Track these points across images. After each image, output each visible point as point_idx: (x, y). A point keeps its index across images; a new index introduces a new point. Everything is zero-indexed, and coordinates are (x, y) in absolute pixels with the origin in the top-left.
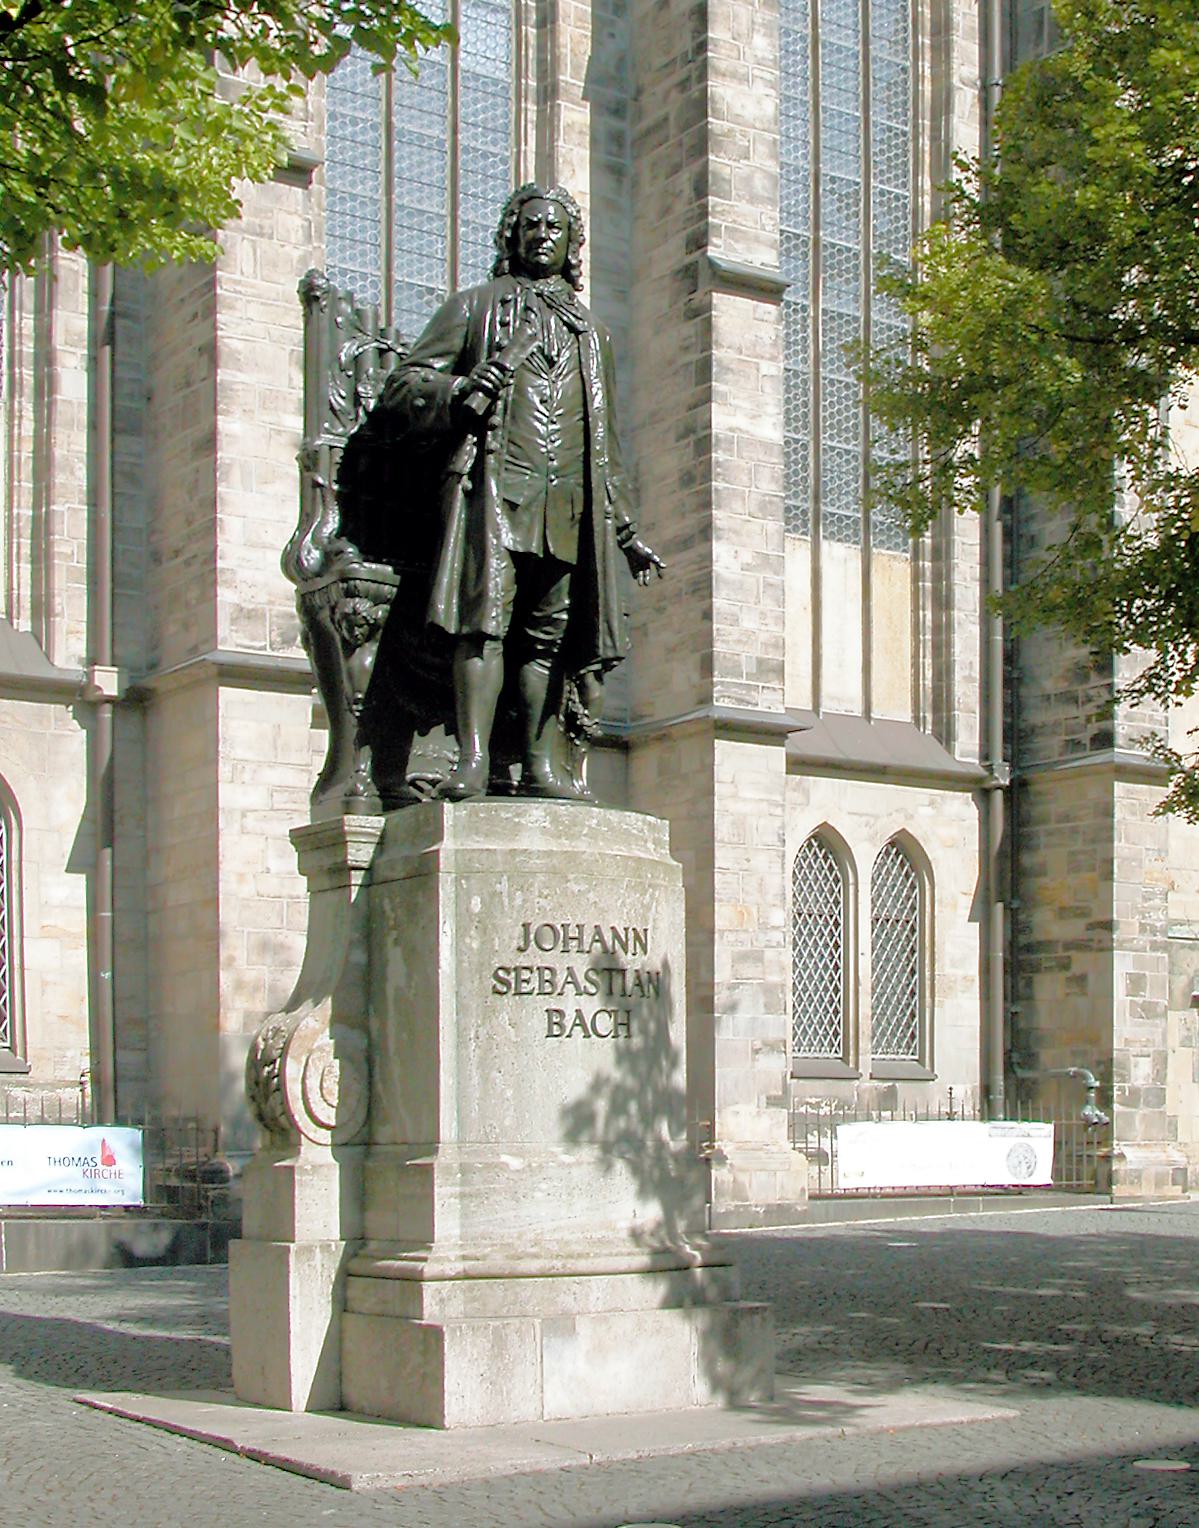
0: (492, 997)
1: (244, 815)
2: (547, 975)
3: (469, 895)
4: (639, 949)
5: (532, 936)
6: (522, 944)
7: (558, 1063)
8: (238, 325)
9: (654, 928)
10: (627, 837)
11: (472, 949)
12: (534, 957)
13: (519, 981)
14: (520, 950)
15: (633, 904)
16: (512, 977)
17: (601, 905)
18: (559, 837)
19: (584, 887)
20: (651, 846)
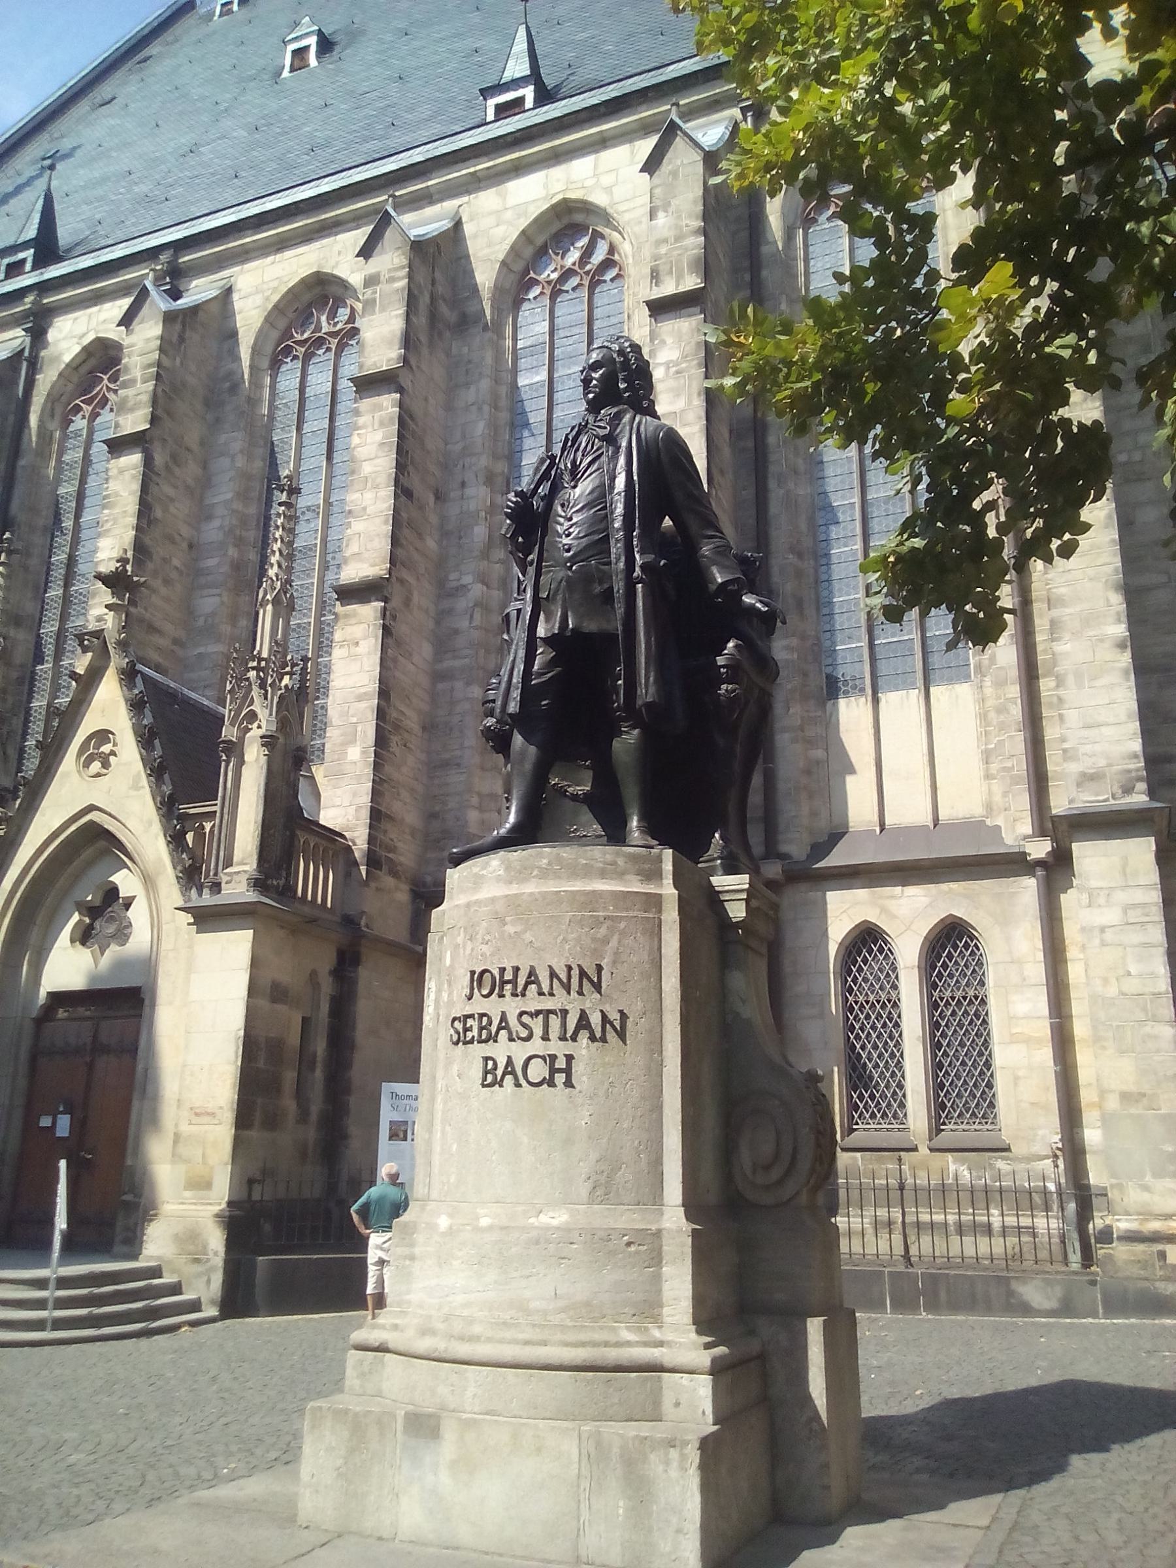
9: (614, 962)
10: (587, 872)
12: (479, 1005)
13: (466, 1030)
15: (578, 940)
18: (511, 883)
19: (519, 928)
20: (633, 878)
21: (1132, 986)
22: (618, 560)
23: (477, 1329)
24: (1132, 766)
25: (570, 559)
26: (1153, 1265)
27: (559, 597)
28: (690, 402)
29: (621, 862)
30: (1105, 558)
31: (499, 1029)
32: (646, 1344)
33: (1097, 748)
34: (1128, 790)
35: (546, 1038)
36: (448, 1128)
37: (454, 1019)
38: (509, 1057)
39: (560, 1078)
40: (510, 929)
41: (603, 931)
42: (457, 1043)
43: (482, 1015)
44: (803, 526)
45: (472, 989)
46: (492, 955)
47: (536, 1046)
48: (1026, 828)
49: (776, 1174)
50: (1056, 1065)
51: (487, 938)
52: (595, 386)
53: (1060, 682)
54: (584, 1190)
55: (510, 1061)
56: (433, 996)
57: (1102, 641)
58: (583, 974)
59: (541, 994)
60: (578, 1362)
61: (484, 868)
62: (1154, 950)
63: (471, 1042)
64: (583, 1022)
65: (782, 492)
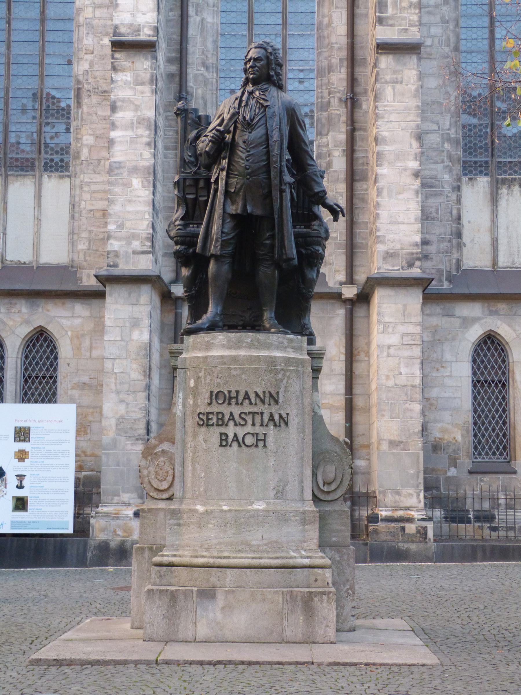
0: (197, 428)
1: (389, 347)
2: (220, 416)
3: (190, 379)
4: (272, 402)
5: (214, 397)
7: (224, 460)
8: (386, 125)
9: (285, 391)
11: (190, 404)
12: (215, 408)
13: (208, 419)
14: (210, 404)
16: (204, 418)
17: (249, 381)
19: (239, 372)
21: (402, 380)
22: (275, 178)
23: (226, 554)
24: (414, 251)
25: (249, 174)
26: (398, 534)
27: (241, 194)
29: (285, 342)
30: (412, 117)
31: (229, 419)
32: (302, 557)
33: (397, 237)
34: (411, 265)
35: (253, 424)
39: (261, 444)
41: (280, 376)
42: (202, 425)
43: (218, 413)
44: (210, 46)
45: (211, 399)
46: (224, 384)
47: (249, 429)
48: (342, 277)
49: (333, 487)
50: (346, 422)
51: (220, 375)
52: (257, 71)
53: (379, 193)
54: (272, 494)
55: (235, 435)
56: (181, 401)
57: (405, 170)
58: (271, 395)
59: (251, 403)
60: (278, 565)
61: (213, 339)
62: (415, 361)
63: (212, 425)
64: (272, 418)
65: (198, 19)
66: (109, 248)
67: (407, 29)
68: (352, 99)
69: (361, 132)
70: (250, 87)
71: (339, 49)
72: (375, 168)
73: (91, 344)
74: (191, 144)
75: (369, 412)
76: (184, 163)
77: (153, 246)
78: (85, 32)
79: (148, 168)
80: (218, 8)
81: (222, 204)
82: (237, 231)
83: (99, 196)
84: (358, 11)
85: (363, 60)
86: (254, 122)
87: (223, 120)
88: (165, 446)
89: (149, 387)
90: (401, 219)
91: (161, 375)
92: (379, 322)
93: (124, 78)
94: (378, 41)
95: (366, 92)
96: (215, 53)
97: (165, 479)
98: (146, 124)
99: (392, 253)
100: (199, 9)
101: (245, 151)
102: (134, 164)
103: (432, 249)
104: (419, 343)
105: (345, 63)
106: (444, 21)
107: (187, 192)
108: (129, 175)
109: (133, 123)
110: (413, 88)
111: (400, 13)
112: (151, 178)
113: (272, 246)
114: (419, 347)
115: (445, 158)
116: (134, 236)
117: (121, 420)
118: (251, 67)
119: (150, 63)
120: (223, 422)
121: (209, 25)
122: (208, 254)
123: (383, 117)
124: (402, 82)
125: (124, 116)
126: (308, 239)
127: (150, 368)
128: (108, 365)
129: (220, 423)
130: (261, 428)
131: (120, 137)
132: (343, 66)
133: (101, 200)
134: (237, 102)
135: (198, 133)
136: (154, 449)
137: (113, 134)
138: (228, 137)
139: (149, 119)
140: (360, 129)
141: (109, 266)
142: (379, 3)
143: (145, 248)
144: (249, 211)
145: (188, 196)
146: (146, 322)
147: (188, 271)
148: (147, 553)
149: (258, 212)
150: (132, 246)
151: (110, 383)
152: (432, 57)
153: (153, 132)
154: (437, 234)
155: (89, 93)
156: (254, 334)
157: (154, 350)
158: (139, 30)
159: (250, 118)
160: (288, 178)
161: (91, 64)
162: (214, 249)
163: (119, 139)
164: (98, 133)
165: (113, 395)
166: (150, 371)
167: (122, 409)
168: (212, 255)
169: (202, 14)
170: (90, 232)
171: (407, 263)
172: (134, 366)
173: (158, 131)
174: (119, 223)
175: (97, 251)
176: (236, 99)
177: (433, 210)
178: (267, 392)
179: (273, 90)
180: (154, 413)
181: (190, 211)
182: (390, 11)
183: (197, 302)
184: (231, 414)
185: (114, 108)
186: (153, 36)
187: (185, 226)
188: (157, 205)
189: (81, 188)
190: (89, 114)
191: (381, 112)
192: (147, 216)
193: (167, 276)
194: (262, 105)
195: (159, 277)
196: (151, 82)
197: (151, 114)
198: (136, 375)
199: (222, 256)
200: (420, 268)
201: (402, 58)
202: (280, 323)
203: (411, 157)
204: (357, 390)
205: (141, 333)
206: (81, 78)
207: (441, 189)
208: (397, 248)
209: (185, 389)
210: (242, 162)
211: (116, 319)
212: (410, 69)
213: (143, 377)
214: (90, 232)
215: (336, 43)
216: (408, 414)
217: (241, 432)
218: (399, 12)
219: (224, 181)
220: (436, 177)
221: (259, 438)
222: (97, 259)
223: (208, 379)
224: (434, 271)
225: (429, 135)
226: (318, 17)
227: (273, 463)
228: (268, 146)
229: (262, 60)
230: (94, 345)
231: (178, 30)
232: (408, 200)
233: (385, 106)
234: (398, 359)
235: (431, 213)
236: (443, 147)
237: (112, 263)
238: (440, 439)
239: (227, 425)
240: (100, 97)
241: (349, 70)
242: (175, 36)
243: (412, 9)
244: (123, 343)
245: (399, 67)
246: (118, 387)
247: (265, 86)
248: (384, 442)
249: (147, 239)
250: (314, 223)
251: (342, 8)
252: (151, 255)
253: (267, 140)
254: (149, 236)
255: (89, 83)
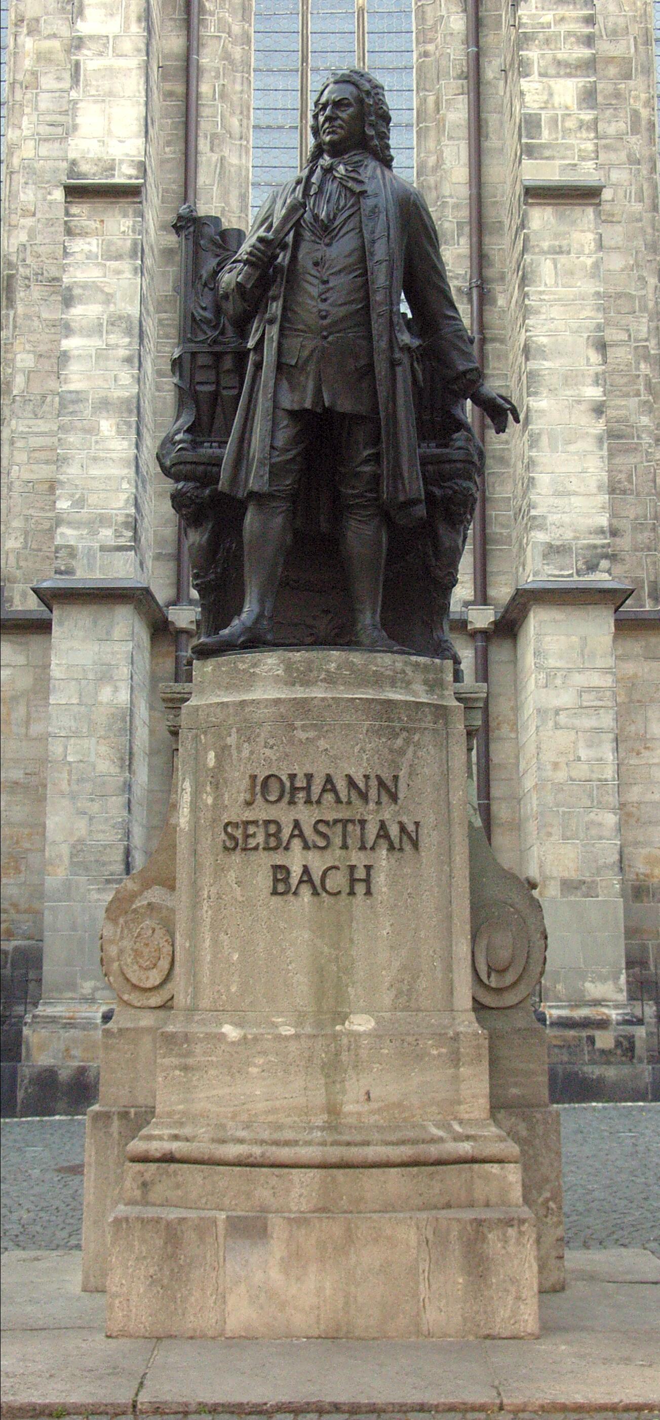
1: (557, 713)
2: (272, 829)
4: (385, 798)
5: (258, 788)
6: (248, 797)
7: (282, 925)
8: (543, 325)
9: (410, 774)
11: (207, 805)
12: (261, 812)
13: (247, 836)
14: (249, 804)
16: (239, 833)
18: (294, 685)
19: (311, 734)
21: (581, 771)
24: (598, 542)
25: (325, 328)
27: (311, 368)
28: (127, 27)
29: (408, 670)
31: (292, 836)
33: (566, 519)
34: (592, 567)
35: (345, 846)
36: (222, 936)
37: (227, 824)
38: (305, 867)
39: (360, 888)
40: (302, 735)
41: (399, 742)
42: (234, 849)
43: (267, 823)
45: (253, 794)
47: (334, 856)
51: (271, 742)
52: (341, 127)
53: (534, 442)
55: (306, 870)
56: (187, 798)
57: (579, 402)
58: (381, 783)
59: (338, 801)
61: (255, 665)
63: (256, 848)
66: (58, 541)
67: (575, 165)
68: (480, 287)
69: (497, 345)
70: (326, 160)
71: (456, 206)
72: (526, 399)
73: (29, 714)
74: (205, 285)
75: (519, 830)
76: (191, 325)
77: (136, 538)
78: (22, 181)
79: (128, 401)
80: (248, 142)
81: (271, 390)
82: (303, 445)
83: (43, 455)
84: (486, 144)
85: (497, 224)
86: (337, 223)
87: (271, 226)
88: (155, 895)
89: (130, 786)
90: (573, 488)
91: (151, 768)
92: (539, 667)
93: (86, 248)
94: (527, 183)
95: (502, 278)
96: (243, 215)
97: (155, 965)
98: (124, 325)
99: (558, 547)
100: (216, 142)
101: (316, 282)
102: (103, 394)
103: (624, 543)
104: (610, 704)
105: (467, 229)
106: (633, 160)
107: (198, 378)
108: (94, 413)
109: (101, 324)
110: (589, 262)
111: (563, 138)
112: (134, 419)
113: (376, 479)
114: (611, 711)
115: (642, 388)
116: (104, 520)
117: (79, 848)
118: (328, 119)
119: (131, 223)
120: (279, 840)
121: (232, 170)
122: (241, 494)
123: (538, 312)
124: (569, 253)
125: (84, 312)
126: (447, 466)
127: (131, 754)
128: (56, 748)
129: (273, 843)
130: (361, 854)
131: (77, 348)
132: (463, 234)
133: (47, 462)
134: (300, 188)
135: (218, 264)
136: (132, 902)
137: (67, 344)
138: (283, 258)
139: (129, 315)
140: (493, 340)
141: (58, 572)
142: (526, 121)
143: (122, 542)
144: (327, 404)
145: (199, 388)
146: (124, 671)
147: (202, 534)
148: (116, 1123)
149: (345, 405)
150: (99, 537)
151: (59, 780)
152: (614, 220)
153: (137, 340)
154: (632, 517)
155: (27, 282)
156: (344, 654)
157: (138, 722)
158: (112, 169)
159: (328, 215)
160: (405, 338)
161: (32, 234)
162: (256, 479)
163: (76, 353)
164: (42, 348)
165: (65, 802)
166: (130, 759)
167: (81, 827)
168: (252, 495)
169: (221, 151)
170: (27, 518)
171: (586, 563)
172: (103, 749)
173: (146, 341)
174: (77, 496)
175: (40, 550)
176: (298, 182)
177: (622, 476)
178: (373, 776)
179: (371, 168)
180: (138, 833)
181: (205, 419)
182: (546, 136)
183: (220, 600)
184: (297, 824)
185: (68, 301)
186: (137, 178)
187: (195, 444)
188: (144, 469)
189: (12, 443)
190: (27, 317)
191: (533, 303)
192: (125, 485)
193: (162, 593)
194: (353, 193)
195: (147, 591)
196: (133, 254)
197: (133, 310)
198: (102, 760)
199: (271, 496)
200: (609, 571)
201: (568, 213)
202: (391, 637)
203: (589, 381)
204: (497, 791)
205: (116, 690)
206: (14, 259)
207: (636, 441)
208: (566, 537)
209: (196, 773)
210: (314, 303)
211: (69, 666)
212: (583, 231)
213: (118, 770)
214: (27, 518)
215: (451, 196)
216: (594, 832)
217: (318, 863)
218: (560, 135)
219: (275, 344)
220: (628, 421)
221: (357, 876)
222: (38, 566)
223: (246, 749)
224: (627, 581)
225: (613, 349)
226: (418, 156)
227: (388, 929)
228: (365, 273)
229: (349, 105)
230: (34, 715)
231: (178, 176)
232: (585, 454)
233: (541, 293)
234: (573, 733)
235: (619, 482)
236: (638, 369)
237: (63, 568)
238: (646, 876)
239: (287, 848)
240: (46, 288)
241: (475, 239)
242: (174, 187)
243: (584, 132)
244: (83, 708)
245: (563, 228)
246: (75, 787)
247: (357, 158)
248: (553, 882)
249: (126, 525)
250: (456, 436)
251: (459, 139)
252: (133, 553)
253: (363, 259)
254: (130, 520)
255: (28, 266)
